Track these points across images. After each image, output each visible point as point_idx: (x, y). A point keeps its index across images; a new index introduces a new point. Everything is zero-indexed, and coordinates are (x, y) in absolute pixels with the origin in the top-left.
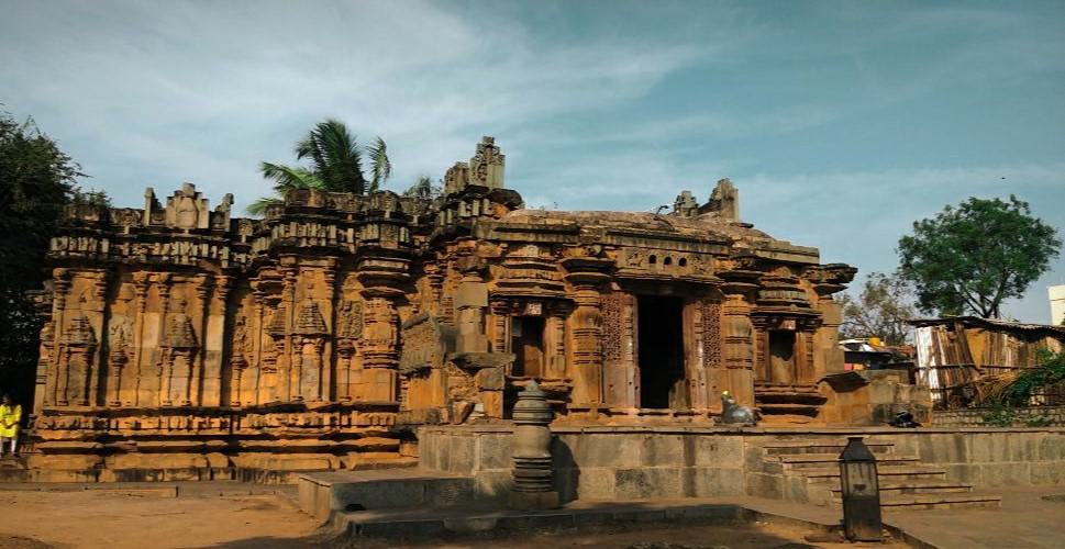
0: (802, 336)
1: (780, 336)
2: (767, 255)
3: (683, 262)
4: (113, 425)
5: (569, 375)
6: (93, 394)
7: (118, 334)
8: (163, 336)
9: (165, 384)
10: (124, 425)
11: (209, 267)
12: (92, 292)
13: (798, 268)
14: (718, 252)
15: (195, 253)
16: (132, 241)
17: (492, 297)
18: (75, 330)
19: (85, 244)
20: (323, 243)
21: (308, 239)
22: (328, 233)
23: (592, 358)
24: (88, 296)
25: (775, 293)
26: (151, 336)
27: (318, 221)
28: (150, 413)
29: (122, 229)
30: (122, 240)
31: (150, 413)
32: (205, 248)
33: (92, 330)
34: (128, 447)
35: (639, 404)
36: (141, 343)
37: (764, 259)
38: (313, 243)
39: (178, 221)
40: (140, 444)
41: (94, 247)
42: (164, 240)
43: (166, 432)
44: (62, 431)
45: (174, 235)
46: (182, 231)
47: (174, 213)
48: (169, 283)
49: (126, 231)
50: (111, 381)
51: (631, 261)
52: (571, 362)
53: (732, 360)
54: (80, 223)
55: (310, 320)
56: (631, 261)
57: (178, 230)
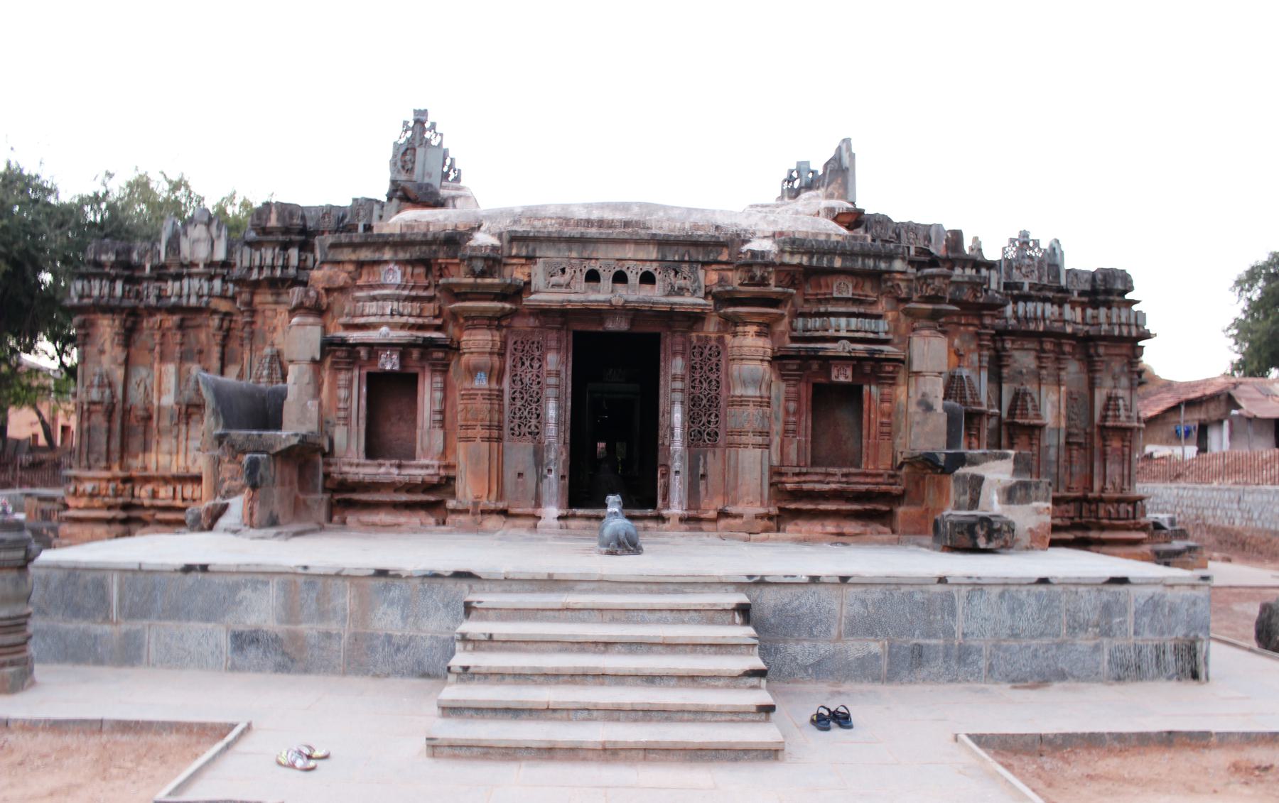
0: (873, 391)
5: (451, 460)
6: (115, 456)
7: (142, 389)
8: (179, 391)
9: (183, 447)
10: (143, 493)
11: (224, 306)
15: (205, 291)
16: (149, 279)
17: (329, 345)
19: (97, 288)
20: (278, 273)
21: (261, 268)
22: (287, 260)
23: (479, 432)
24: (108, 346)
25: (818, 322)
27: (273, 244)
28: (166, 480)
29: (144, 268)
30: (139, 281)
31: (166, 480)
32: (217, 284)
33: (110, 385)
35: (565, 500)
36: (159, 399)
38: (266, 273)
39: (192, 253)
40: (160, 516)
41: (106, 290)
42: (178, 277)
46: (197, 265)
48: (181, 327)
50: (136, 443)
51: (554, 280)
54: (98, 264)
55: (265, 372)
56: (554, 280)
57: (193, 264)
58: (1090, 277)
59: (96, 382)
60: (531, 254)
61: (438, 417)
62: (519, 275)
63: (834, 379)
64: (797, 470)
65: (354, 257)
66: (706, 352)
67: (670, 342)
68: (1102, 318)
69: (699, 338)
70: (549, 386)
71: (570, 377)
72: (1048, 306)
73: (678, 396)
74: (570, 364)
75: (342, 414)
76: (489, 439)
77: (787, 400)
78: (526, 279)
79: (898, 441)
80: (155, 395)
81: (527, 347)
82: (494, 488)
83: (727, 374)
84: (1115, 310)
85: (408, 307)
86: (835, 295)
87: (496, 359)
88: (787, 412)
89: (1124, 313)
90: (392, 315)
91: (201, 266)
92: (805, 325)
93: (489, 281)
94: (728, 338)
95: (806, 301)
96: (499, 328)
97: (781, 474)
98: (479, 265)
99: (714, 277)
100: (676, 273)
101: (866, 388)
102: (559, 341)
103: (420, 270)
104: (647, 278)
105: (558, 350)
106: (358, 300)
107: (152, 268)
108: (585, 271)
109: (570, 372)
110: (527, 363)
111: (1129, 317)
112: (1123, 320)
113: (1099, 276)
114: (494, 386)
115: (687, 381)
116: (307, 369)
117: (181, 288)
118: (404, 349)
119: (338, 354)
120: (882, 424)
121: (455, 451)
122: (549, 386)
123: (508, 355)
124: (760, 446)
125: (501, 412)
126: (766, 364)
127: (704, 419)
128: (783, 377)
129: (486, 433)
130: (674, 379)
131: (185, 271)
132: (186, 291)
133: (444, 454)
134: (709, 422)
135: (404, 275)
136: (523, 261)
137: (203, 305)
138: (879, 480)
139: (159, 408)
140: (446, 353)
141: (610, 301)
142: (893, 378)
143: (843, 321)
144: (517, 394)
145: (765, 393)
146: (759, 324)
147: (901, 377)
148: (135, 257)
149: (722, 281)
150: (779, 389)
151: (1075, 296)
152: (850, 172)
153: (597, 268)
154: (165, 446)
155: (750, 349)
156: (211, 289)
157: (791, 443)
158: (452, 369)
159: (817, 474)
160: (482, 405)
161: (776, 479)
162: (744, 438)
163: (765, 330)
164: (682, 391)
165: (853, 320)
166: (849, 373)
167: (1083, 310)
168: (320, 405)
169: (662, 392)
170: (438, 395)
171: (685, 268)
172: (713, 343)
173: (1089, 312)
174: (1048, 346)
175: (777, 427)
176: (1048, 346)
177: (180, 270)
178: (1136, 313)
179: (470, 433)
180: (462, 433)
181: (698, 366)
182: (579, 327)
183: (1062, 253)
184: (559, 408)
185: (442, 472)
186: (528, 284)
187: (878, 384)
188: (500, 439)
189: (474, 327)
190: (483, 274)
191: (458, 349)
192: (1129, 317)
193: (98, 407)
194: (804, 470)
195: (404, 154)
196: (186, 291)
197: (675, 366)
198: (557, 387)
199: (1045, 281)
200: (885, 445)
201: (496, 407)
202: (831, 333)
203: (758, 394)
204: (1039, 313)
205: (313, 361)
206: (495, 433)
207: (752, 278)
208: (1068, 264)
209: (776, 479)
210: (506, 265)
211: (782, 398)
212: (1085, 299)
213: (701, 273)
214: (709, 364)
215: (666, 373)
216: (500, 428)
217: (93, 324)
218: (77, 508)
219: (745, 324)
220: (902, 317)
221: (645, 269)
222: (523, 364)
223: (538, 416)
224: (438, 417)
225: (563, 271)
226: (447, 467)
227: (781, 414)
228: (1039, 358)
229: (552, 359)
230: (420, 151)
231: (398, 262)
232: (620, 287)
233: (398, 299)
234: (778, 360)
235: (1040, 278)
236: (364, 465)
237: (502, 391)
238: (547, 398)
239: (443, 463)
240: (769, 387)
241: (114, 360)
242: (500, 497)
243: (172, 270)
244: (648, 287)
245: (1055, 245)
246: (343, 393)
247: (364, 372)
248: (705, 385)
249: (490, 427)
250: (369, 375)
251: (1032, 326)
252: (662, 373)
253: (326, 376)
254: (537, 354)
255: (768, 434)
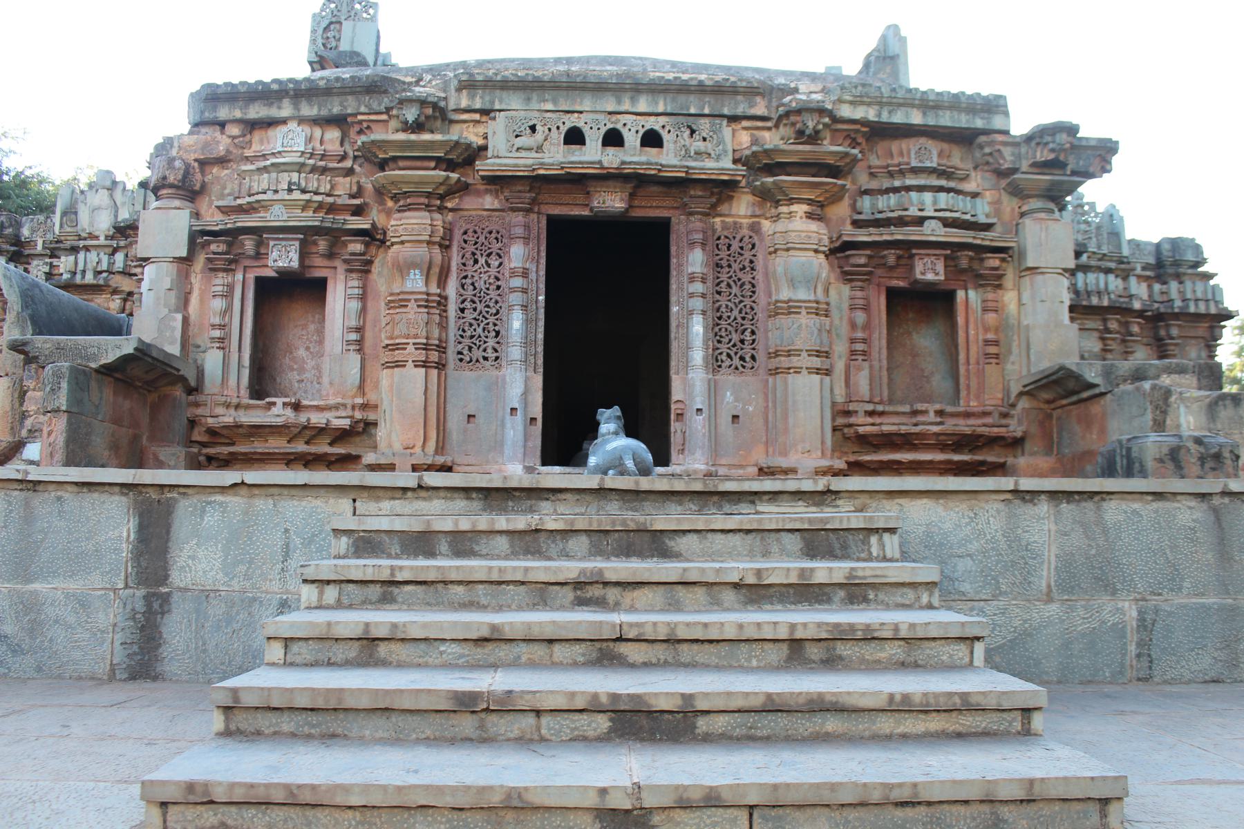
0: (969, 298)
1: (917, 293)
2: (871, 114)
3: (652, 139)
5: (372, 397)
13: (964, 138)
14: (740, 111)
15: (105, 267)
17: (198, 239)
25: (893, 199)
37: (864, 122)
39: (91, 224)
42: (74, 250)
45: (81, 243)
46: (97, 238)
47: (87, 212)
49: (40, 247)
51: (519, 142)
52: (373, 367)
53: (777, 354)
56: (519, 142)
58: (1153, 249)
60: (488, 107)
61: (353, 336)
62: (472, 136)
63: (919, 276)
64: (870, 407)
65: (238, 114)
66: (735, 245)
67: (684, 228)
68: (1174, 294)
69: (725, 226)
70: (513, 290)
71: (543, 279)
72: (1111, 277)
73: (698, 304)
74: (543, 261)
75: (217, 333)
76: (425, 364)
77: (852, 308)
78: (481, 142)
79: (1009, 367)
81: (482, 239)
82: (433, 435)
83: (766, 274)
84: (1188, 285)
85: (313, 182)
86: (914, 163)
87: (436, 250)
88: (853, 326)
89: (1199, 287)
90: (290, 190)
91: (102, 238)
92: (873, 205)
93: (427, 137)
94: (766, 225)
95: (872, 175)
96: (441, 209)
97: (848, 413)
98: (411, 114)
99: (745, 138)
100: (693, 132)
101: (960, 294)
102: (527, 227)
103: (333, 134)
104: (652, 139)
105: (526, 240)
106: (242, 175)
108: (564, 129)
109: (542, 273)
110: (482, 261)
111: (1205, 292)
112: (1199, 295)
113: (1166, 246)
114: (434, 289)
115: (709, 284)
116: (173, 268)
117: (76, 263)
118: (307, 236)
119: (213, 247)
120: (987, 342)
121: (377, 386)
122: (513, 290)
123: (455, 248)
124: (818, 371)
125: (443, 326)
126: (822, 256)
127: (735, 337)
128: (847, 276)
129: (421, 356)
130: (692, 279)
131: (81, 243)
132: (81, 266)
133: (361, 388)
134: (742, 341)
135: (310, 139)
136: (477, 116)
137: (101, 282)
138: (989, 420)
140: (367, 245)
141: (600, 162)
142: (1000, 277)
143: (928, 197)
144: (467, 304)
145: (820, 295)
146: (810, 202)
147: (1009, 280)
148: (26, 232)
149: (755, 141)
150: (841, 294)
151: (1139, 271)
152: (902, 59)
153: (580, 124)
155: (794, 244)
156: (111, 264)
157: (859, 369)
158: (376, 268)
159: (897, 413)
160: (413, 313)
161: (841, 421)
162: (795, 359)
163: (819, 211)
164: (703, 296)
165: (943, 195)
166: (940, 267)
167: (1150, 287)
168: (186, 321)
169: (673, 299)
170: (355, 305)
171: (704, 125)
172: (745, 232)
173: (1157, 287)
174: (1113, 325)
175: (840, 349)
176: (1113, 325)
177: (75, 243)
178: (1213, 287)
179: (398, 355)
180: (386, 357)
181: (724, 263)
182: (557, 211)
183: (1121, 219)
184: (527, 322)
185: (358, 415)
186: (484, 148)
187: (978, 286)
188: (441, 366)
189: (408, 208)
190: (418, 127)
191: (383, 242)
192: (1205, 292)
194: (880, 408)
195: (326, 29)
196: (81, 266)
197: (690, 262)
198: (524, 291)
199: (1105, 250)
200: (991, 370)
201: (437, 318)
202: (913, 212)
203: (812, 298)
204: (1102, 285)
205: (180, 260)
206: (434, 356)
207: (800, 133)
208: (1132, 231)
209: (841, 421)
210: (452, 122)
211: (846, 305)
212: (1148, 273)
213: (727, 132)
214: (735, 266)
215: (680, 273)
216: (442, 348)
219: (791, 201)
220: (1005, 198)
221: (648, 127)
222: (476, 262)
223: (498, 333)
224: (353, 336)
225: (533, 129)
226: (364, 407)
227: (844, 330)
228: (1103, 339)
229: (517, 254)
230: (347, 26)
231: (302, 121)
232: (611, 150)
233: (300, 167)
234: (840, 250)
235: (1099, 247)
236: (248, 407)
237: (446, 298)
238: (510, 308)
239: (359, 401)
240: (827, 291)
242: (440, 449)
243: (68, 244)
244: (654, 151)
245: (1113, 211)
246: (218, 304)
247: (251, 276)
248: (735, 290)
249: (426, 347)
250: (261, 282)
251: (1095, 301)
252: (673, 273)
253: (196, 280)
254: (495, 246)
255: (827, 355)
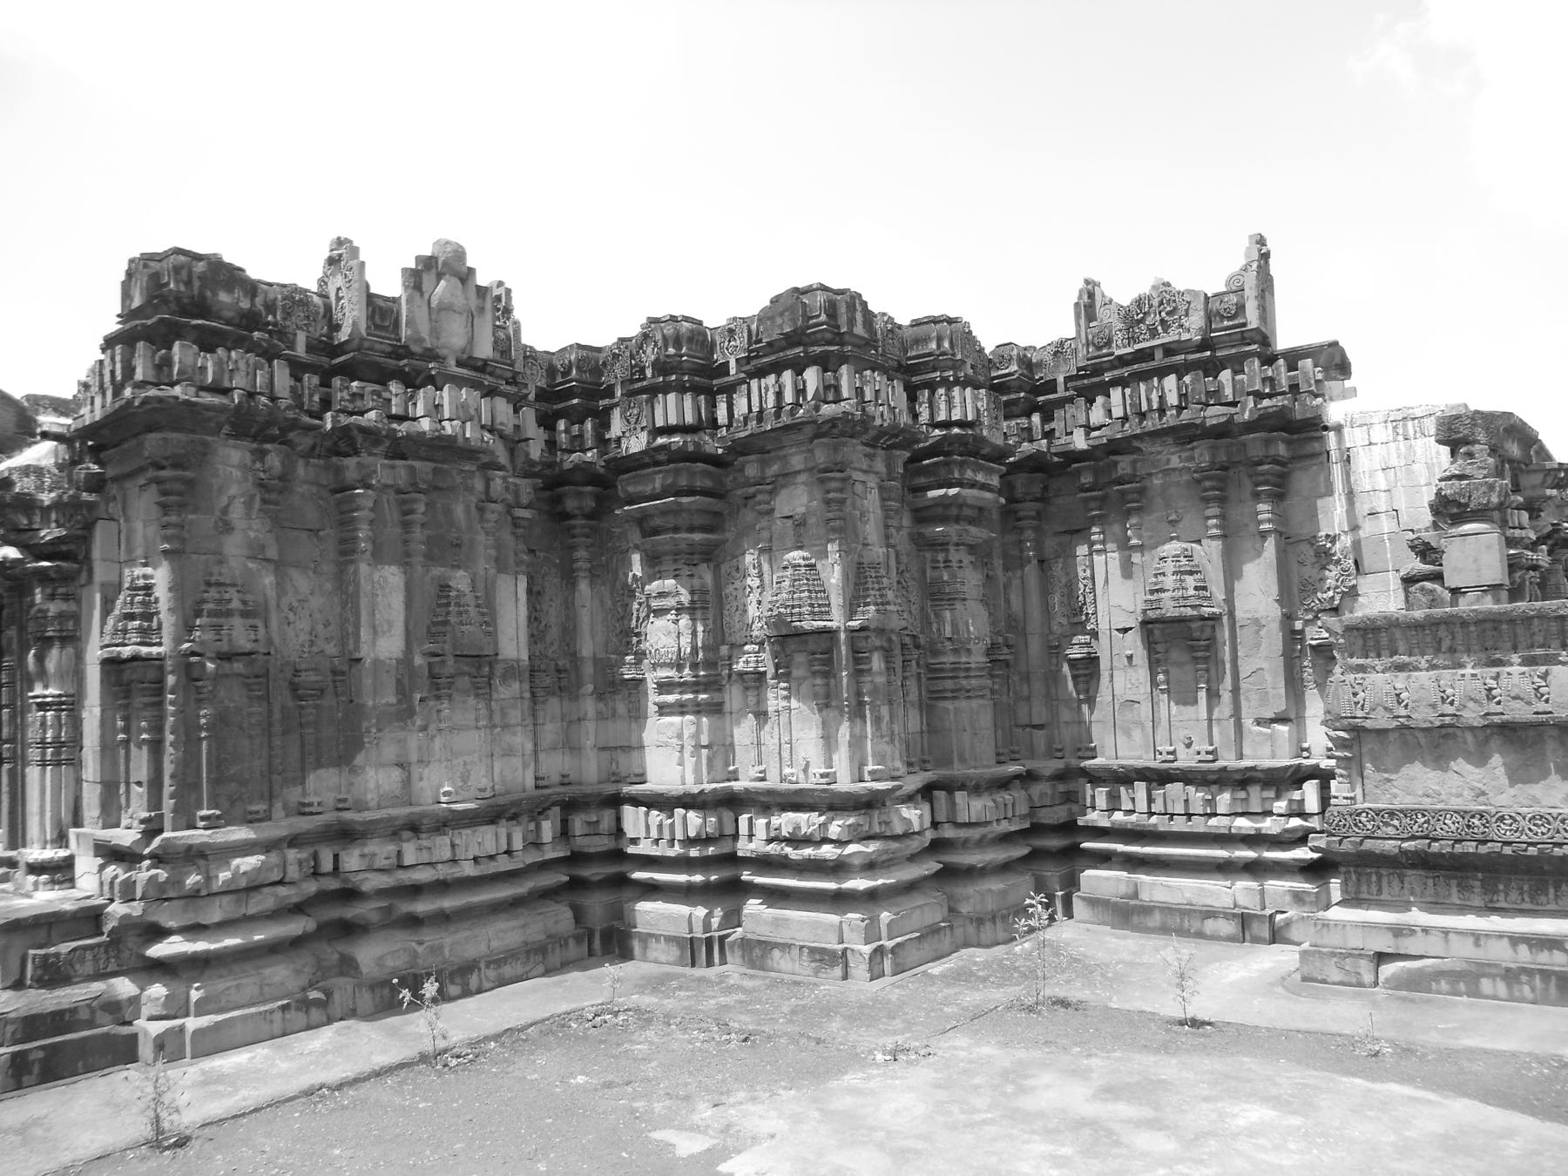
4: (327, 865)
12: (248, 505)
18: (229, 614)
24: (237, 513)
26: (390, 624)
34: (375, 917)
39: (435, 332)
40: (422, 907)
43: (469, 870)
44: (226, 899)
57: (431, 355)
59: (236, 604)
80: (365, 634)
107: (310, 348)
139: (377, 662)
154: (389, 751)
193: (238, 666)
217: (203, 454)
218: (193, 930)
241: (256, 552)
